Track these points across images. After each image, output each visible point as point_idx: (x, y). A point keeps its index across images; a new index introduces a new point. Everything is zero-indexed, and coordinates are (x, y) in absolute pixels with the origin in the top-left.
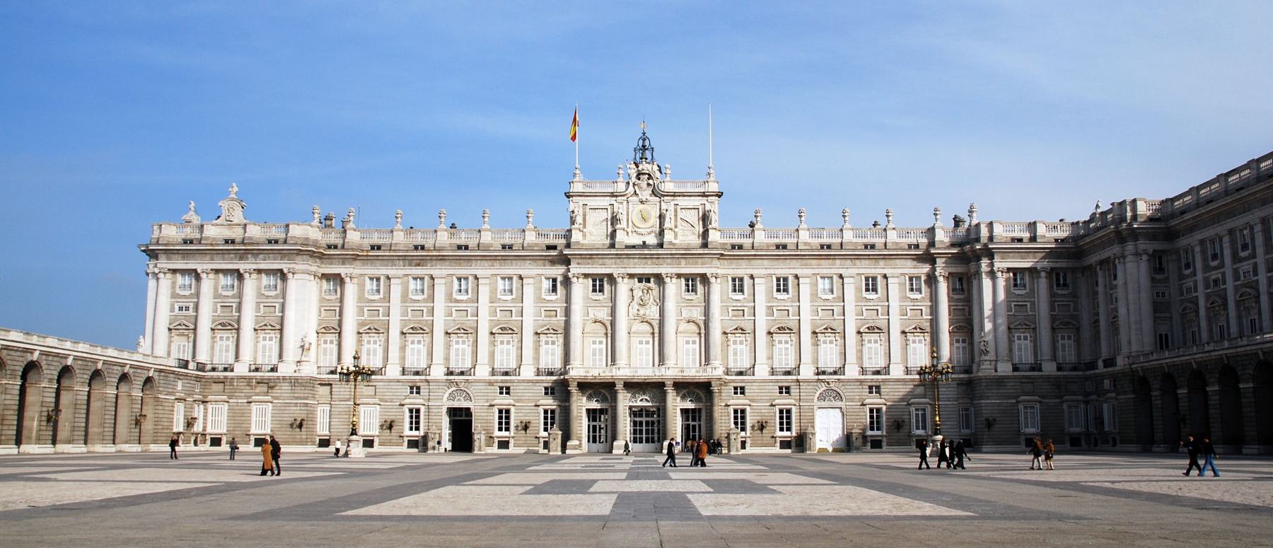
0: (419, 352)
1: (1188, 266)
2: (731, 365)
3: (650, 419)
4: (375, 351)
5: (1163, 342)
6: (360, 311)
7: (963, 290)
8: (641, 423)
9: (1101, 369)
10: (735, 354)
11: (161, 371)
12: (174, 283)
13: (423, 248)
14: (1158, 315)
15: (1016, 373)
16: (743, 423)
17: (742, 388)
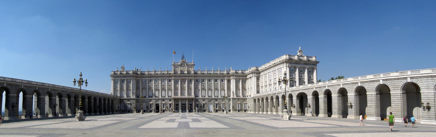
2: (196, 95)
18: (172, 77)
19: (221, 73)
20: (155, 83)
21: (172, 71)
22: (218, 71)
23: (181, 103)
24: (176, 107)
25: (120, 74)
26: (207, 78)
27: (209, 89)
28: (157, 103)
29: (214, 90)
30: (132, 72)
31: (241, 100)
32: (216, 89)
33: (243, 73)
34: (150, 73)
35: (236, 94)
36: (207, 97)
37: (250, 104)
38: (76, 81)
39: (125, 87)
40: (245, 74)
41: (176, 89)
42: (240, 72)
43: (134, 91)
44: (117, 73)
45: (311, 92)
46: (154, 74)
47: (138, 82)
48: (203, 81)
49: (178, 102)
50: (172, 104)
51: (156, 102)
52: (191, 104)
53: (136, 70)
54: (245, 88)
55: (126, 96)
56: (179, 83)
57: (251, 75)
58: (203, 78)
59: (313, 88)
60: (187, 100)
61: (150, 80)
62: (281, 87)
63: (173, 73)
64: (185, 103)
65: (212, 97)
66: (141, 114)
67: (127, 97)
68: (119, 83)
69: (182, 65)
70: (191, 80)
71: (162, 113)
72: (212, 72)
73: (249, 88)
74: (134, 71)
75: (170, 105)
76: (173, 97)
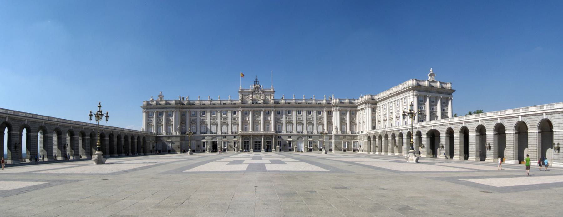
0: (204, 128)
1: (379, 110)
2: (277, 130)
3: (259, 144)
4: (194, 128)
5: (374, 128)
6: (190, 119)
7: (330, 114)
8: (257, 145)
9: (360, 133)
10: (278, 128)
11: (146, 135)
12: (148, 115)
13: (204, 104)
14: (373, 122)
15: (342, 134)
16: (280, 145)
17: (280, 136)
18: (238, 107)
19: (317, 102)
20: (211, 116)
21: (238, 100)
22: (312, 100)
23: (252, 141)
24: (245, 145)
25: (157, 104)
26: (296, 109)
27: (299, 123)
28: (214, 140)
29: (307, 124)
30: (174, 102)
31: (349, 138)
32: (310, 123)
33: (352, 103)
34: (203, 102)
35: (341, 130)
36: (295, 132)
37: (362, 142)
38: (92, 114)
39: (164, 121)
40: (354, 104)
41: (244, 123)
42: (347, 101)
43: (178, 127)
44: (151, 104)
45: (444, 129)
46: (209, 103)
47: (184, 115)
48: (289, 113)
49: (248, 139)
50: (238, 141)
51: (212, 139)
52: (269, 142)
53: (181, 99)
54: (354, 123)
55: (174, 132)
56: (251, 115)
57: (363, 105)
58: (289, 109)
59: (447, 124)
60: (263, 137)
61: (203, 112)
62: (406, 122)
63: (240, 103)
64: (259, 140)
65: (304, 134)
66: (189, 154)
67: (166, 134)
68: (154, 117)
69: (254, 92)
70: (269, 111)
71: (222, 153)
72: (303, 101)
73: (361, 123)
74: (178, 100)
75: (235, 143)
76: (239, 133)
